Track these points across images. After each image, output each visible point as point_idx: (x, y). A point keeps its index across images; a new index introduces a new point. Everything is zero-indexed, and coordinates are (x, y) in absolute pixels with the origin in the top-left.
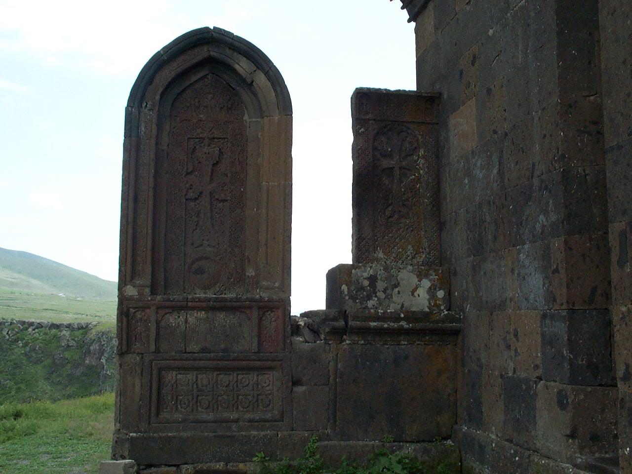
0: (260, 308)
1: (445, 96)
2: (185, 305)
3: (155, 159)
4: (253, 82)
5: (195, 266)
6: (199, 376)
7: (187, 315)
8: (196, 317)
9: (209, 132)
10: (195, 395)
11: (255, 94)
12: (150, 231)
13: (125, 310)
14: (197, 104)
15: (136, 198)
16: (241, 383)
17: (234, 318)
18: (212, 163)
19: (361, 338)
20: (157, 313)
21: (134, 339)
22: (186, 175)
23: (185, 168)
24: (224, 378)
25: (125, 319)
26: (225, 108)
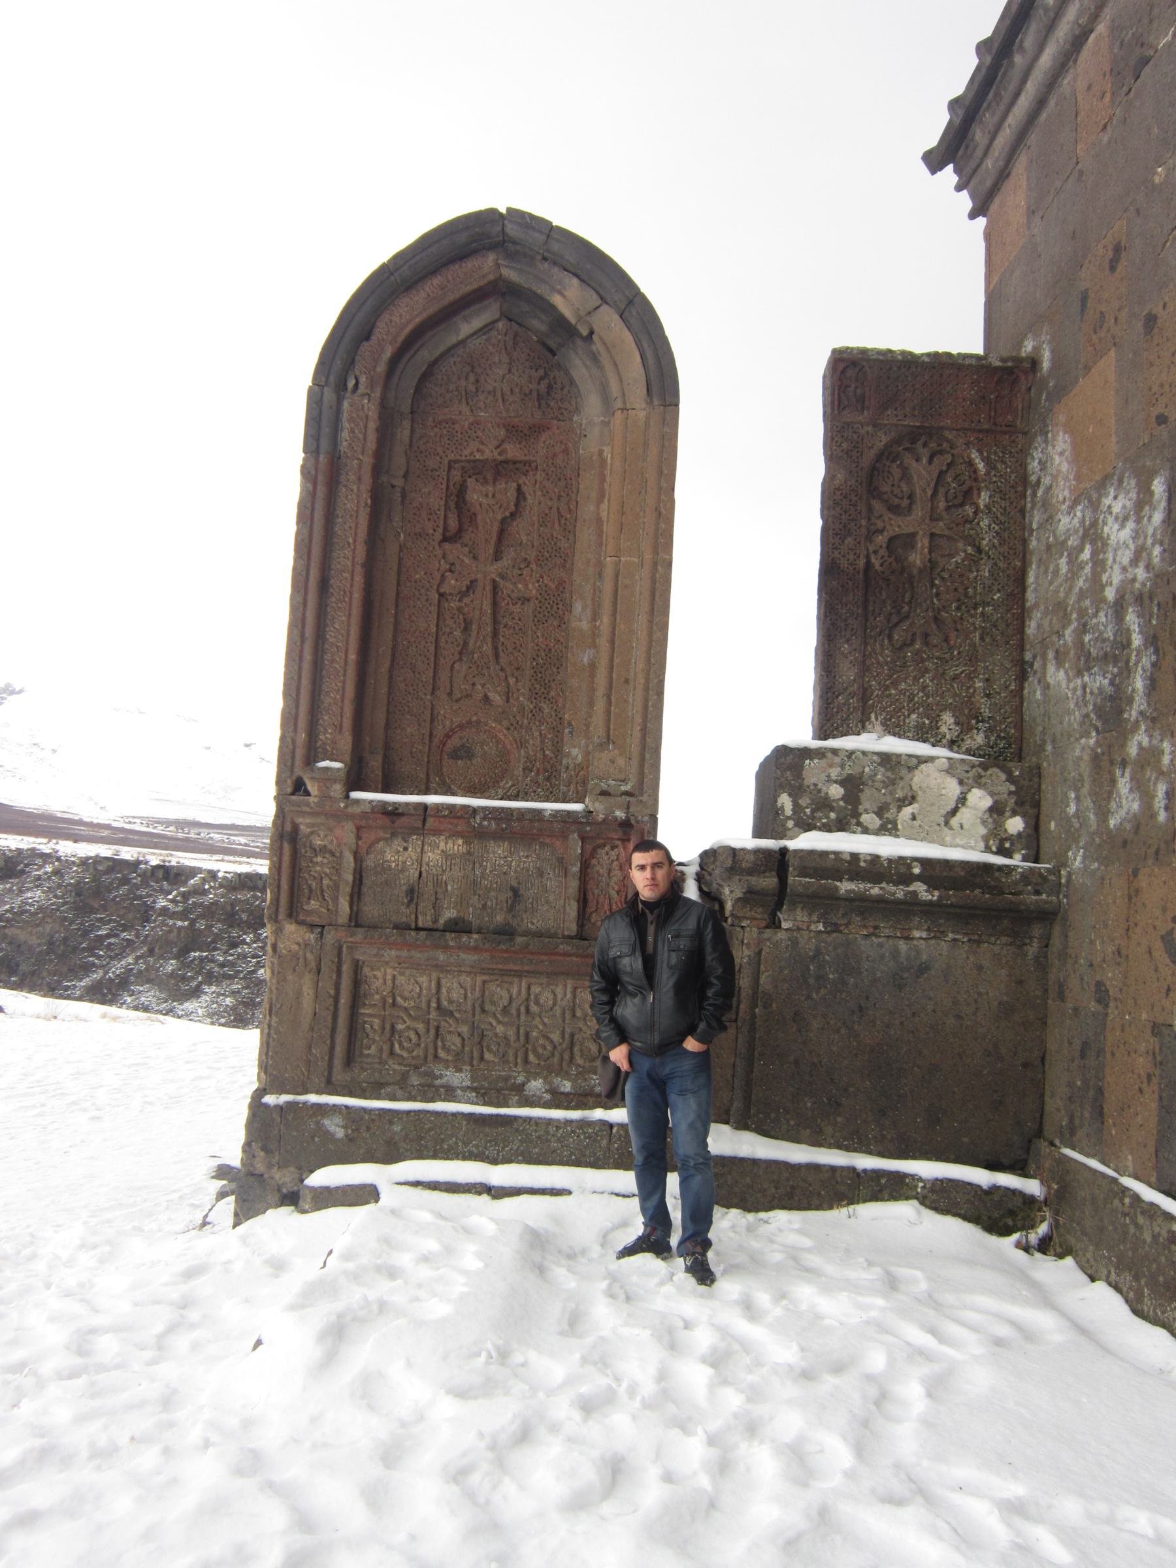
1: (1046, 365)
3: (369, 501)
4: (592, 333)
5: (455, 742)
6: (443, 981)
10: (433, 1024)
12: (353, 657)
13: (288, 827)
14: (472, 388)
15: (324, 585)
16: (537, 1003)
17: (527, 857)
18: (499, 517)
19: (815, 918)
20: (359, 838)
24: (500, 993)
25: (287, 847)
26: (535, 394)
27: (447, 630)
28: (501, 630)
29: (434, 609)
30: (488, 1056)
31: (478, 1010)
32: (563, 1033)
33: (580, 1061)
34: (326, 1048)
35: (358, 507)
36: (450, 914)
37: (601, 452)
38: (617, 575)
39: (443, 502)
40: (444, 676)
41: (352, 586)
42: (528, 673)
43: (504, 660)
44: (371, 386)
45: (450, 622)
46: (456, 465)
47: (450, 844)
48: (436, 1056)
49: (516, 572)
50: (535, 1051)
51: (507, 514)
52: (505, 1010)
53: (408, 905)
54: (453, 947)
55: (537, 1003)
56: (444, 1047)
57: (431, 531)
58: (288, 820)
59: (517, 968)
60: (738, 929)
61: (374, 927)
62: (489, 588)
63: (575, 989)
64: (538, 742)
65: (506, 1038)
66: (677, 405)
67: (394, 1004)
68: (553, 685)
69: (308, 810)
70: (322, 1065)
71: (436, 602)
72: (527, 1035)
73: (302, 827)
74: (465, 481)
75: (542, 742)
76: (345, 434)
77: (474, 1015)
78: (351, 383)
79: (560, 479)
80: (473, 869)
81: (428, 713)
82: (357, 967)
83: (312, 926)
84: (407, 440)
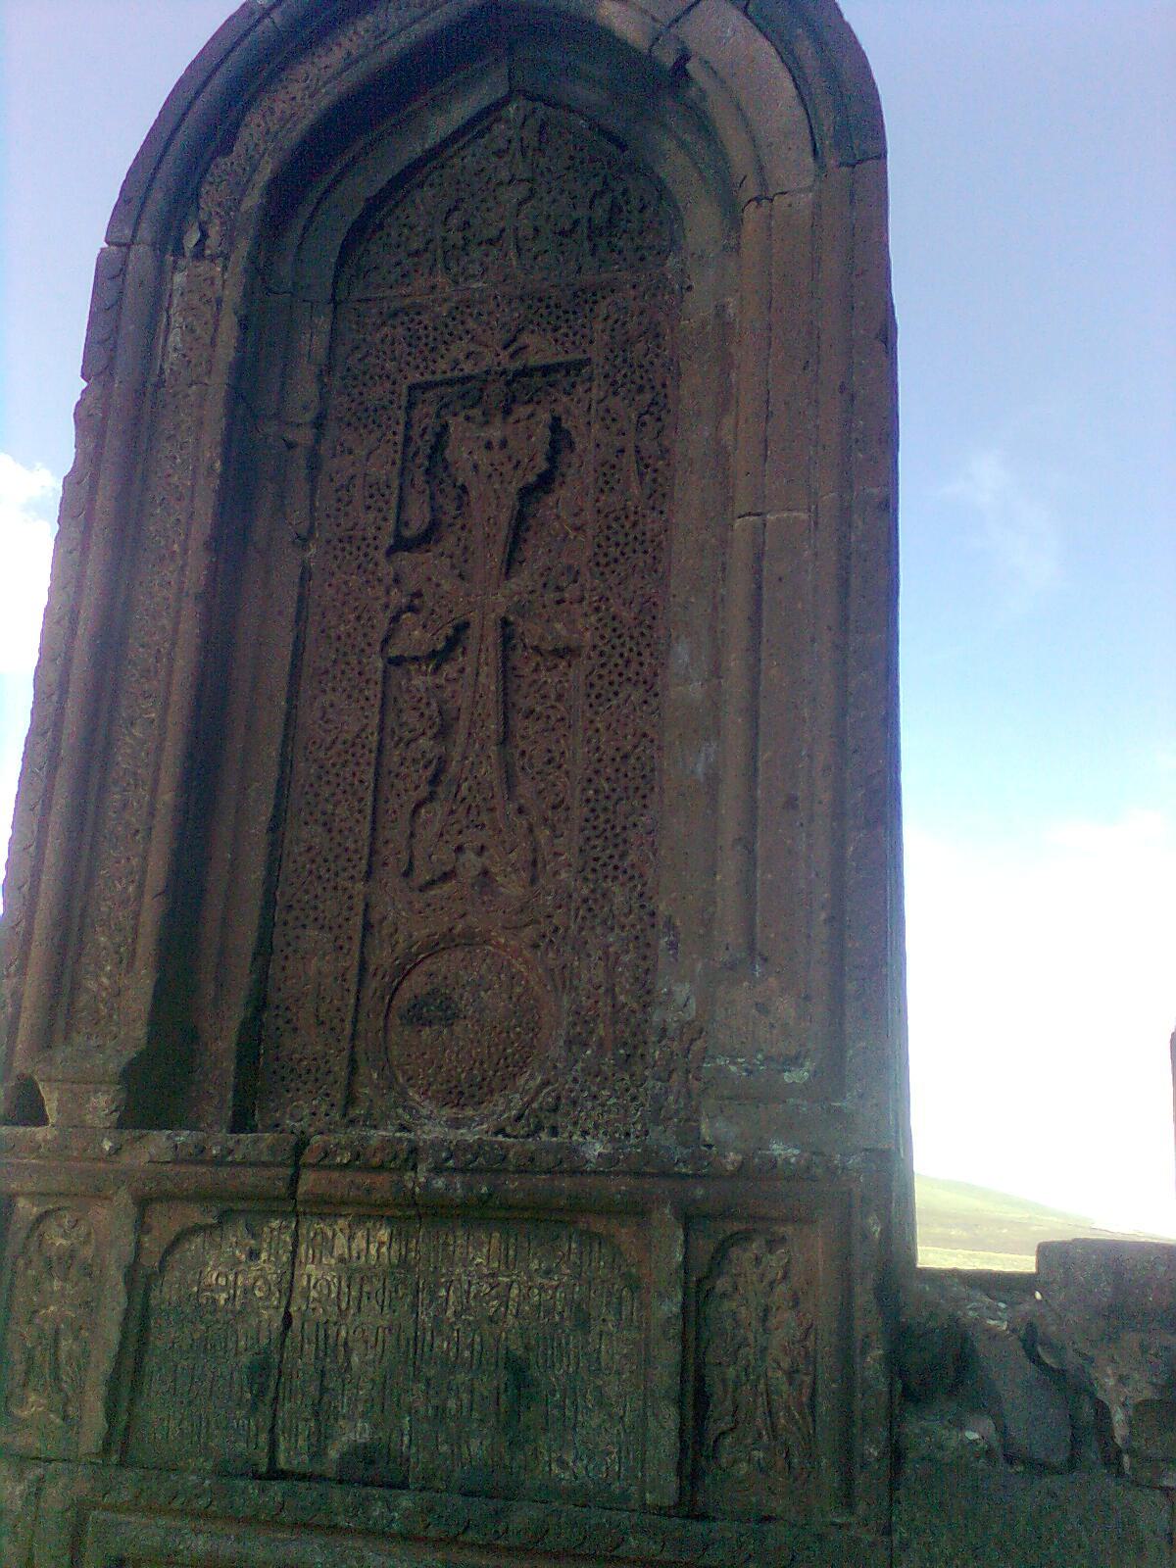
0: (689, 1219)
2: (281, 1188)
3: (218, 464)
4: (684, 57)
7: (296, 1245)
8: (342, 1260)
9: (505, 348)
11: (704, 127)
12: (167, 797)
14: (456, 237)
17: (548, 1273)
18: (514, 487)
20: (142, 1226)
21: (20, 1368)
22: (391, 551)
23: (392, 522)
26: (583, 229)
27: (407, 736)
28: (519, 723)
29: (374, 691)
35: (194, 478)
36: (353, 1432)
37: (721, 309)
38: (759, 557)
39: (396, 470)
40: (395, 833)
41: (174, 644)
42: (579, 812)
43: (525, 789)
44: (229, 237)
45: (410, 718)
46: (430, 395)
47: (360, 1242)
49: (551, 596)
51: (532, 478)
53: (254, 1407)
54: (348, 1530)
57: (371, 531)
62: (493, 637)
64: (599, 975)
66: (882, 156)
68: (631, 835)
71: (379, 676)
73: (22, 1203)
74: (445, 427)
75: (610, 973)
76: (175, 338)
78: (192, 238)
79: (641, 389)
80: (414, 1306)
81: (358, 920)
84: (321, 355)
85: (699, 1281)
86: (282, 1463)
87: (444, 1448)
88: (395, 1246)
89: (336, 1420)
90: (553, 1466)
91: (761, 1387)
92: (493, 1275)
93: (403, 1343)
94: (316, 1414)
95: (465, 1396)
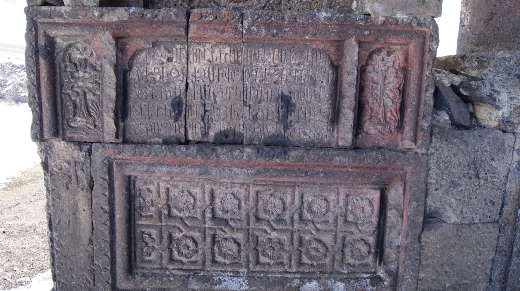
6: (217, 192)
8: (209, 61)
10: (209, 233)
13: (42, 42)
16: (310, 210)
25: (42, 61)
30: (263, 259)
31: (252, 219)
32: (335, 237)
33: (351, 261)
34: (108, 260)
36: (218, 126)
47: (217, 53)
48: (214, 262)
50: (308, 253)
52: (280, 220)
53: (176, 119)
55: (310, 210)
56: (221, 253)
58: (41, 32)
59: (292, 180)
60: (511, 135)
61: (143, 143)
63: (347, 196)
65: (280, 243)
67: (170, 215)
69: (61, 21)
70: (106, 274)
72: (301, 240)
73: (59, 40)
77: (248, 224)
80: (242, 79)
82: (129, 183)
83: (80, 144)
85: (362, 66)
86: (190, 137)
87: (258, 130)
88: (232, 55)
89: (212, 122)
90: (302, 134)
91: (382, 104)
92: (276, 66)
93: (238, 93)
94: (203, 120)
95: (265, 112)
